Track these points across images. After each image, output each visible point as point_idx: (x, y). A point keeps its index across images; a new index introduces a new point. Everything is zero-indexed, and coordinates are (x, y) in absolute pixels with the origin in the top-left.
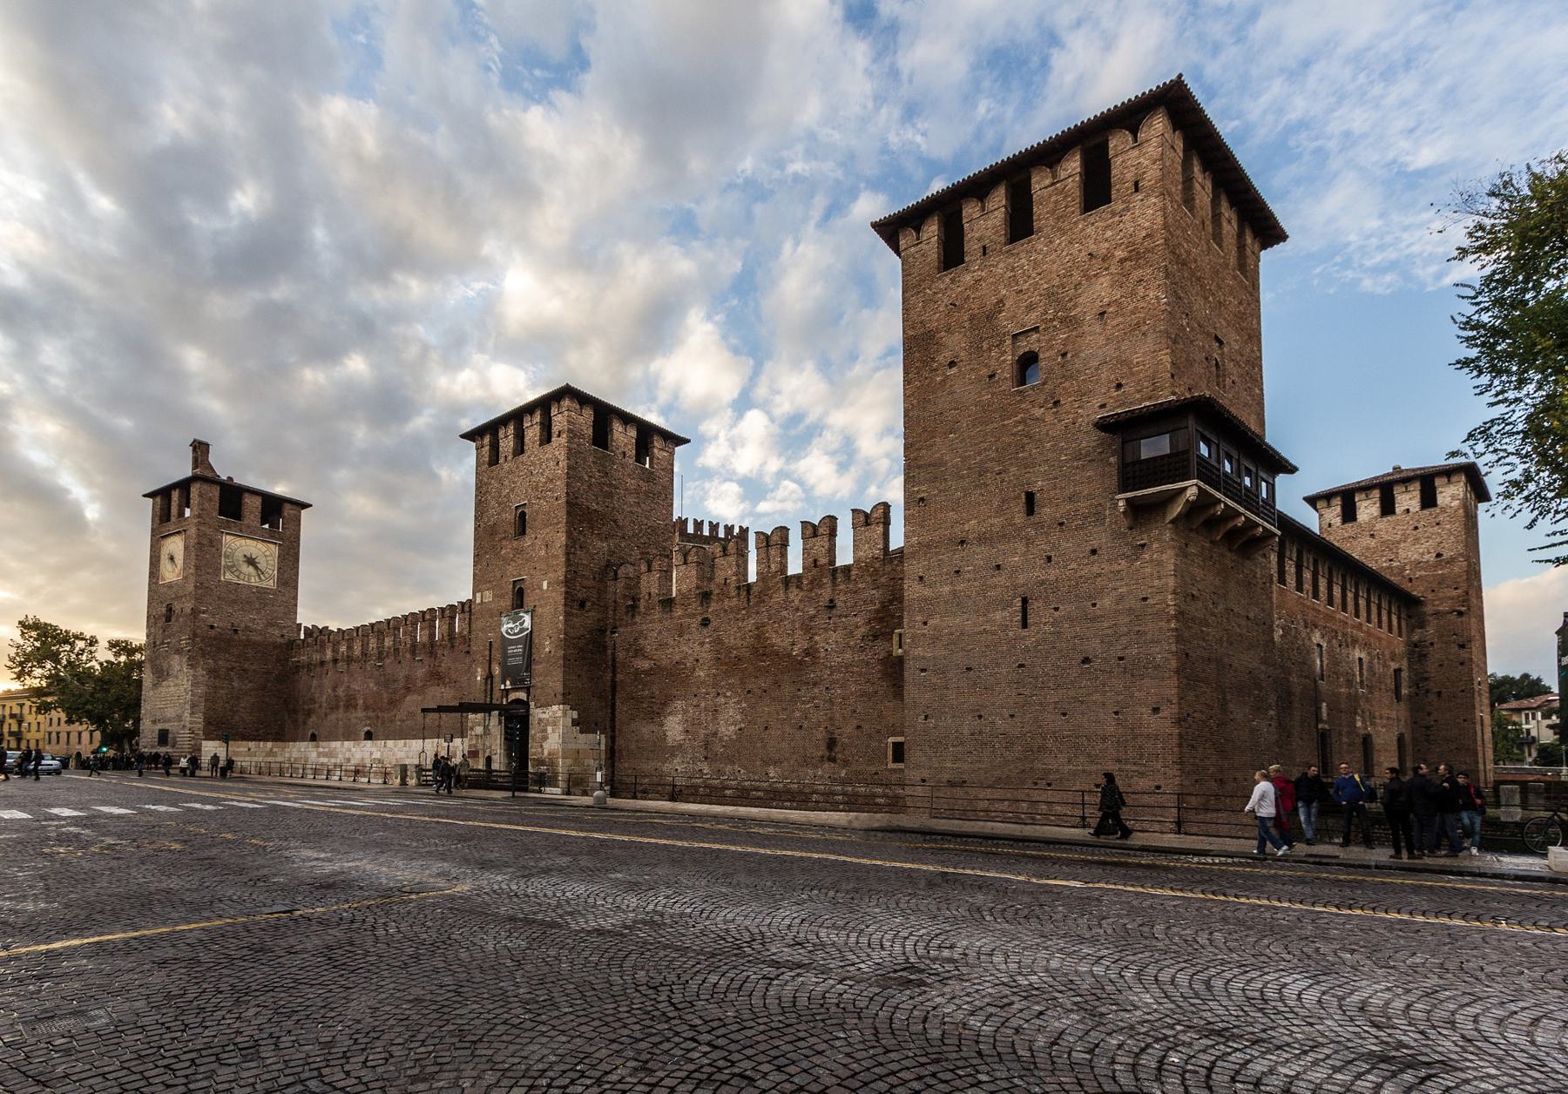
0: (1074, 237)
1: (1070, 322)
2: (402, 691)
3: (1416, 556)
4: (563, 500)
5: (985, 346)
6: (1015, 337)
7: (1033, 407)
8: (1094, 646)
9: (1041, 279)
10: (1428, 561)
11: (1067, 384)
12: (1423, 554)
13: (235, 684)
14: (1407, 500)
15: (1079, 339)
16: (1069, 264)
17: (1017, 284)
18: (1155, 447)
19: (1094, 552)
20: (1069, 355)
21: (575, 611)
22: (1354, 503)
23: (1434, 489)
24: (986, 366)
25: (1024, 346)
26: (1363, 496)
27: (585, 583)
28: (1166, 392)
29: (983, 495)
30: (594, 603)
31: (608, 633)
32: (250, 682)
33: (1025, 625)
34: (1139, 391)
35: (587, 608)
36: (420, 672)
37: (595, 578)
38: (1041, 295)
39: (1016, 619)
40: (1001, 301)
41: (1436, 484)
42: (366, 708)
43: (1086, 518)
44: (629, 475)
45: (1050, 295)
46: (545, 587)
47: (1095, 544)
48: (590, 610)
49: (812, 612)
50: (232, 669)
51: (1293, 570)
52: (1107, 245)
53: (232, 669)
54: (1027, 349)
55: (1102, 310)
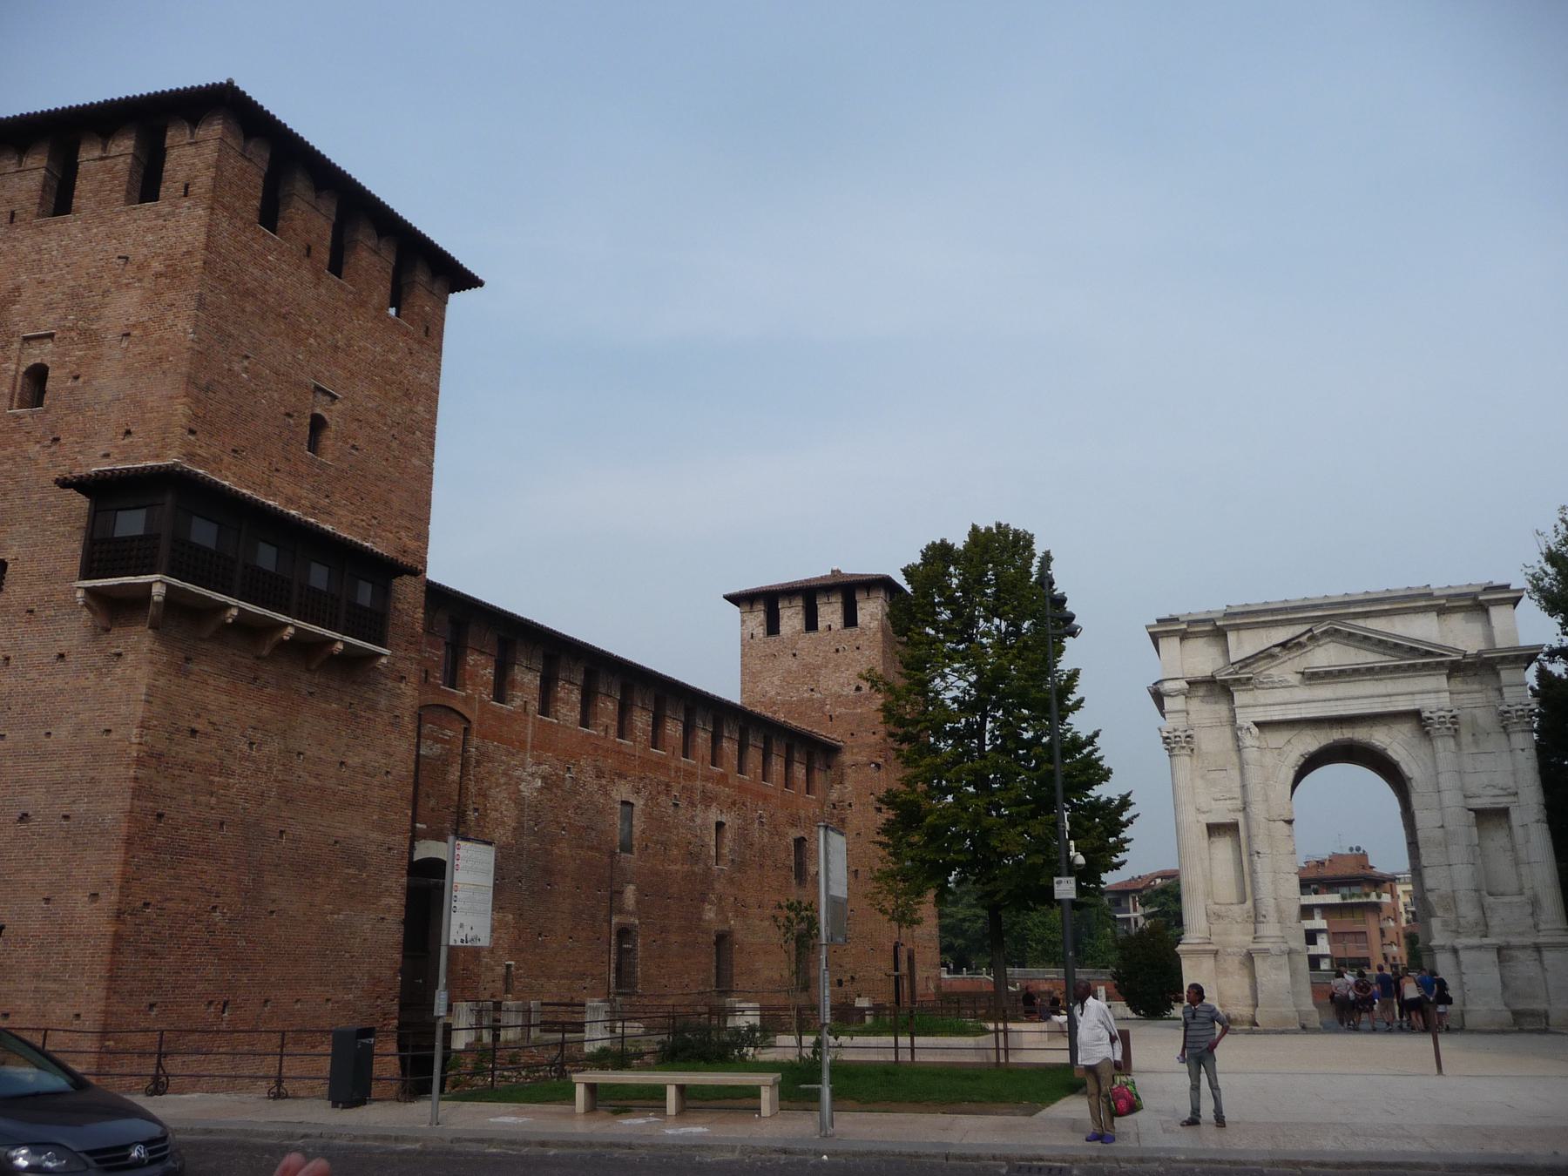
0: (113, 230)
1: (90, 338)
3: (836, 688)
6: (27, 339)
7: (28, 440)
9: (68, 273)
10: (847, 696)
11: (72, 418)
12: (843, 685)
14: (830, 613)
16: (102, 263)
17: (41, 271)
18: (131, 523)
19: (61, 656)
20: (81, 380)
22: (778, 610)
23: (855, 603)
25: (40, 354)
26: (786, 603)
28: (174, 453)
34: (147, 445)
38: (64, 293)
40: (18, 289)
41: (857, 598)
43: (60, 606)
45: (74, 295)
47: (64, 646)
52: (145, 251)
55: (126, 331)
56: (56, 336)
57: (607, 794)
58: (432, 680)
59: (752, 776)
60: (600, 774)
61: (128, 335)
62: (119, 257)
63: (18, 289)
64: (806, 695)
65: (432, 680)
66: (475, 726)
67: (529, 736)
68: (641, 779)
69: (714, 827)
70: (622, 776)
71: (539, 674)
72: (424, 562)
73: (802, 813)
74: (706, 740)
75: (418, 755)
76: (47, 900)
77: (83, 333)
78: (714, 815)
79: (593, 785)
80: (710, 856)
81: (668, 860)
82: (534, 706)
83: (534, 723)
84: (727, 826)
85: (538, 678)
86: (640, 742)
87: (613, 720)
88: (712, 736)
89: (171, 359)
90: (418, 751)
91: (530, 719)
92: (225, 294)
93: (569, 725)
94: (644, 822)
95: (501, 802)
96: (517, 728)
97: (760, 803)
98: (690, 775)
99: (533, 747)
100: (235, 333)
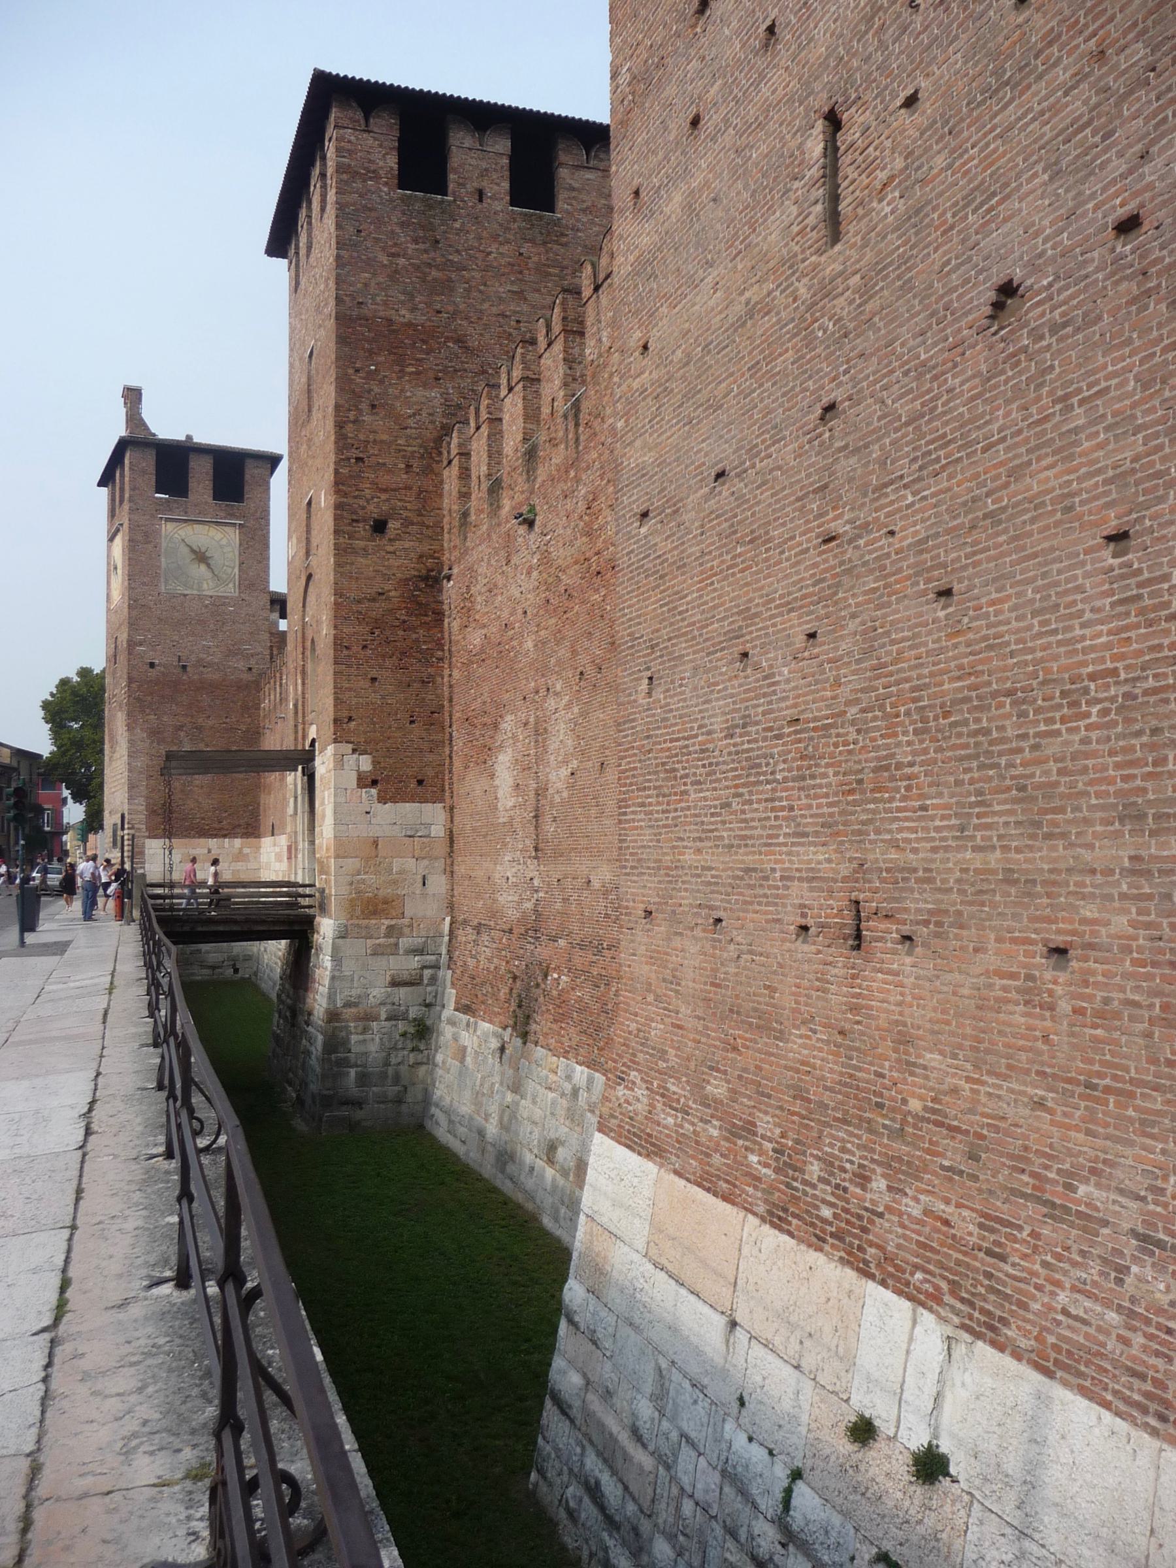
21: (362, 543)
27: (385, 480)
30: (407, 523)
37: (408, 466)
39: (811, 220)
44: (495, 237)
48: (398, 538)
50: (180, 728)
53: (180, 728)
76: (1118, 538)
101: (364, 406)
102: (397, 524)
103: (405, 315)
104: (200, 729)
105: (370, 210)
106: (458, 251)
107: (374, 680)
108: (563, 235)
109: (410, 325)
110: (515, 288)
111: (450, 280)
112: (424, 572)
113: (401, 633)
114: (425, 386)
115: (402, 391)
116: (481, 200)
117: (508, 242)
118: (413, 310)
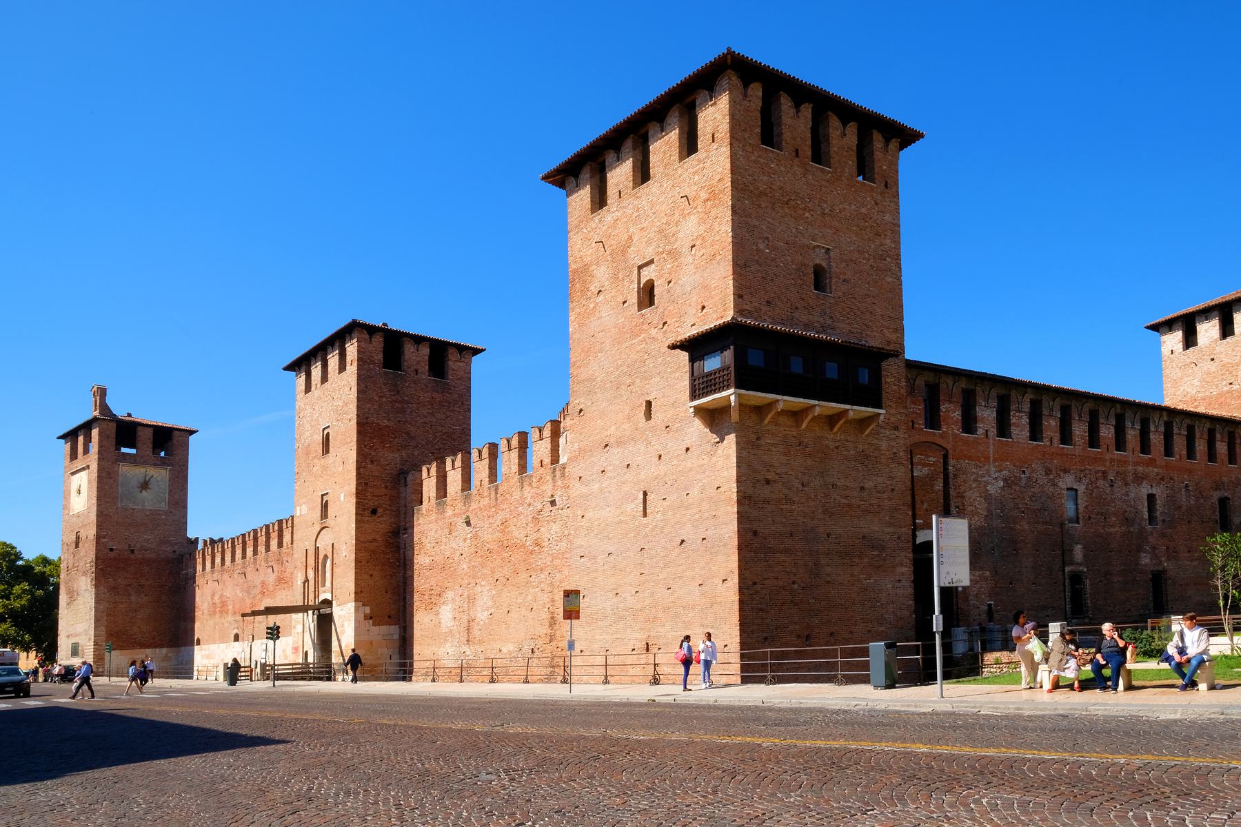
1: (674, 254)
2: (260, 596)
4: (354, 421)
5: (621, 276)
8: (687, 532)
13: (133, 598)
15: (678, 268)
20: (672, 282)
21: (367, 518)
24: (622, 293)
25: (647, 274)
29: (619, 405)
31: (401, 535)
32: (146, 595)
33: (645, 515)
35: (378, 514)
36: (272, 578)
38: (655, 232)
42: (235, 613)
45: (659, 232)
46: (342, 499)
48: (381, 516)
49: (540, 507)
50: (129, 585)
51: (1025, 420)
54: (648, 278)
56: (655, 260)
57: (1055, 485)
58: (917, 426)
59: (1178, 457)
60: (1048, 472)
61: (694, 246)
62: (682, 197)
63: (630, 237)
64: (1225, 388)
65: (917, 426)
66: (950, 452)
67: (991, 452)
68: (1081, 471)
69: (1146, 498)
70: (1066, 471)
71: (995, 410)
72: (903, 347)
73: (1225, 479)
74: (1135, 436)
75: (913, 476)
77: (669, 253)
78: (1145, 490)
79: (1043, 480)
80: (1142, 519)
81: (1108, 525)
82: (993, 432)
83: (994, 445)
84: (1157, 496)
85: (995, 413)
86: (1079, 445)
87: (1056, 432)
88: (1140, 432)
89: (721, 253)
90: (912, 475)
91: (991, 441)
92: (747, 199)
93: (1020, 441)
94: (1086, 501)
95: (974, 500)
96: (982, 449)
97: (1186, 476)
98: (1123, 462)
99: (995, 460)
100: (757, 224)
101: (368, 461)
102: (381, 510)
103: (386, 423)
104: (142, 586)
105: (371, 377)
106: (408, 396)
107: (371, 575)
108: (450, 389)
109: (387, 426)
110: (430, 411)
111: (404, 407)
112: (392, 530)
113: (382, 555)
114: (393, 452)
115: (384, 454)
116: (417, 374)
117: (428, 392)
118: (389, 420)
